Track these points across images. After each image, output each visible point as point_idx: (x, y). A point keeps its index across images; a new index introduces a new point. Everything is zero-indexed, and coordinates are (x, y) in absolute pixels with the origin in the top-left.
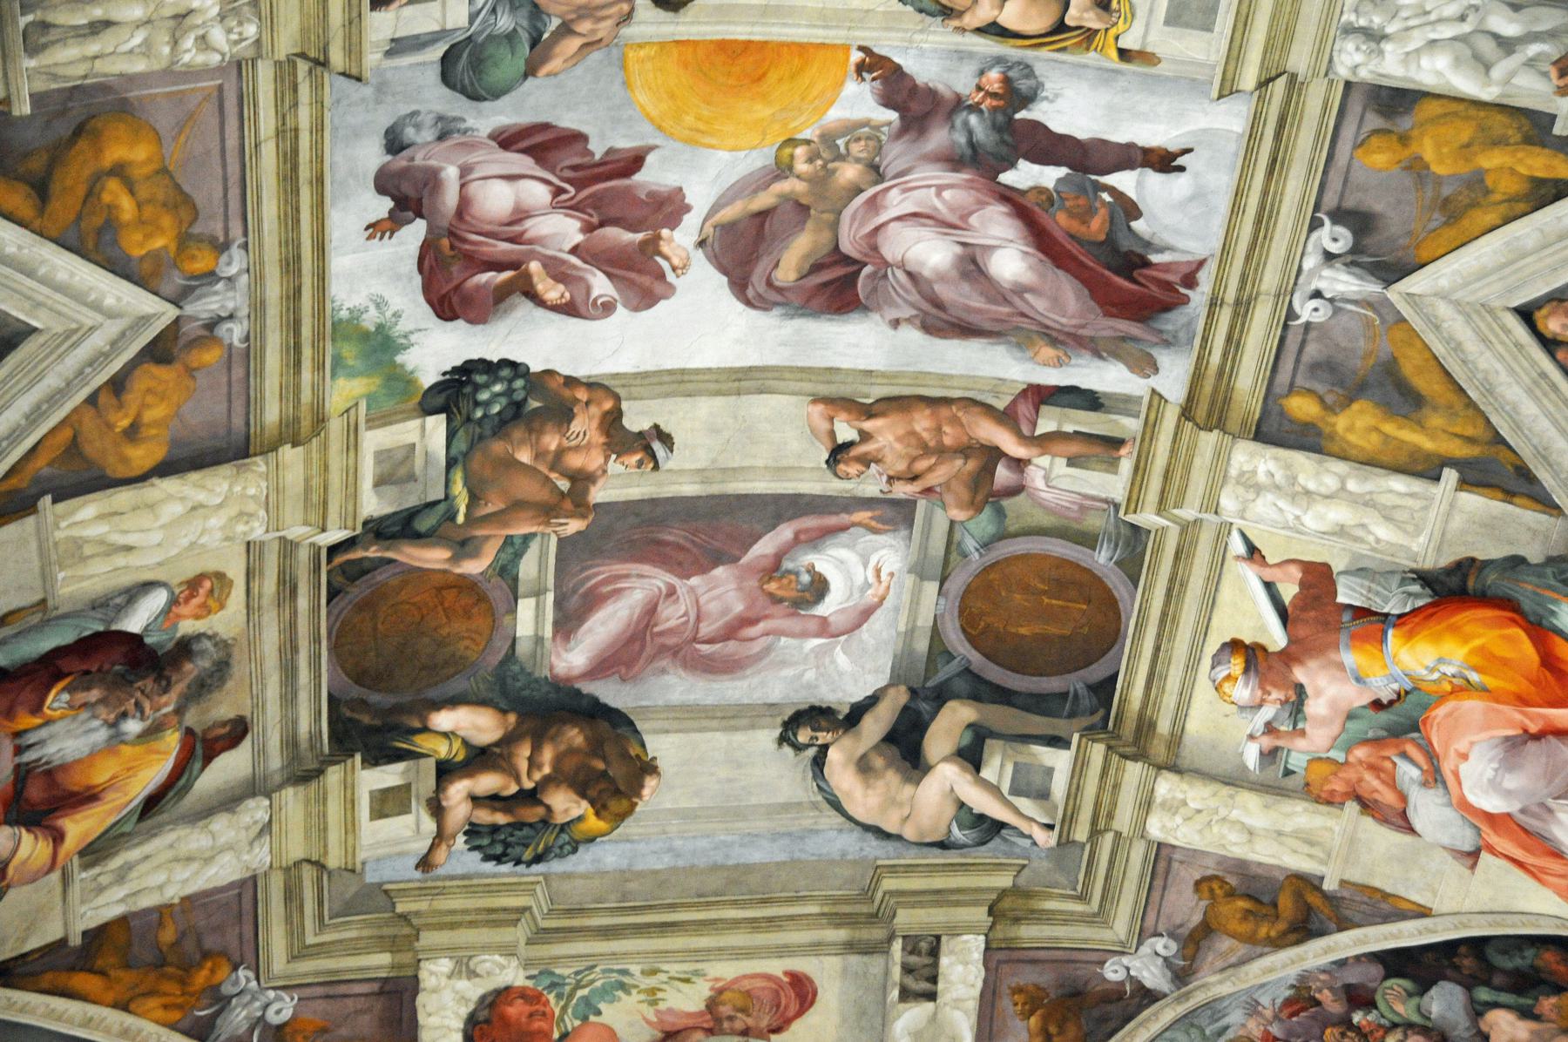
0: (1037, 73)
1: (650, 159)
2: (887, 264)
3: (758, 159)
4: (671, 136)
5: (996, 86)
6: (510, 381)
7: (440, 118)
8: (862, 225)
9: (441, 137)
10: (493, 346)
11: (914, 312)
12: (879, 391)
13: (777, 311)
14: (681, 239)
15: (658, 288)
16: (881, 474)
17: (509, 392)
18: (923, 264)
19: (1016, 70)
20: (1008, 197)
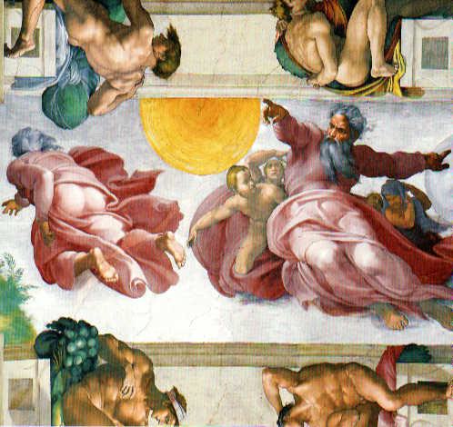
7: (42, 136)
9: (43, 149)
12: (304, 361)
14: (179, 239)
15: (169, 276)
18: (316, 259)
20: (357, 203)
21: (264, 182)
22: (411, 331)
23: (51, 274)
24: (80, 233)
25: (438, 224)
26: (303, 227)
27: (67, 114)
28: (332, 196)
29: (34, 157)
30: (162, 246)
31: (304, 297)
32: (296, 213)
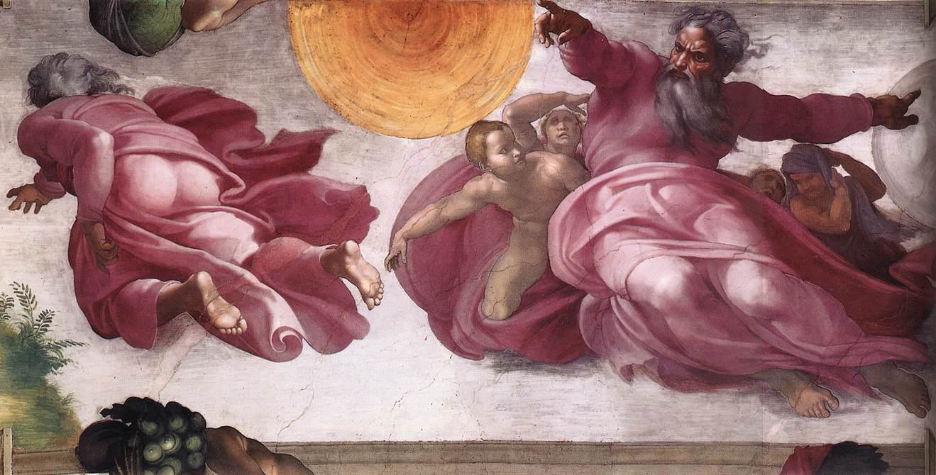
0: (739, 22)
1: (328, 147)
2: (609, 293)
3: (447, 149)
4: (347, 119)
5: (697, 43)
6: (184, 437)
7: (90, 67)
8: (573, 239)
9: (93, 92)
10: (160, 382)
11: (649, 357)
13: (488, 361)
15: (349, 323)
17: (182, 454)
18: (650, 290)
19: (715, 21)
20: (730, 187)
21: (544, 150)
22: (845, 419)
23: (109, 319)
24: (168, 245)
25: (900, 225)
26: (624, 230)
27: (142, 30)
28: (681, 175)
29: (73, 107)
30: (335, 267)
31: (625, 359)
32: (608, 206)
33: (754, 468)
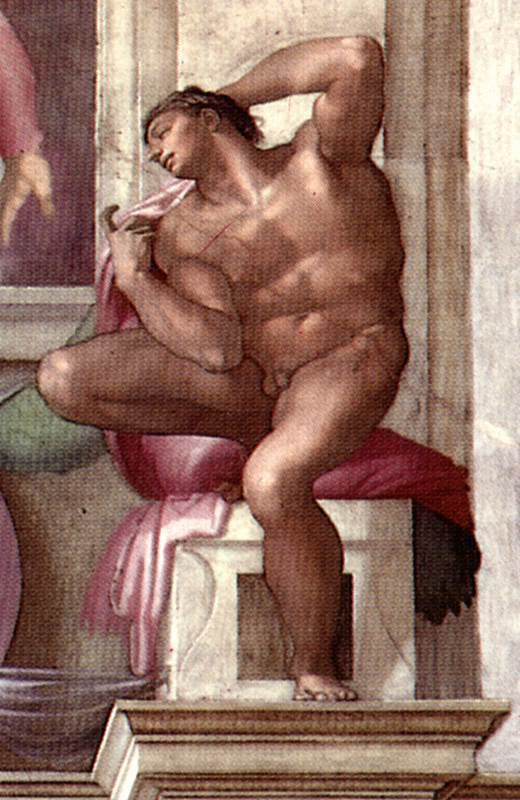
16: (163, 203)
33: (423, 400)
